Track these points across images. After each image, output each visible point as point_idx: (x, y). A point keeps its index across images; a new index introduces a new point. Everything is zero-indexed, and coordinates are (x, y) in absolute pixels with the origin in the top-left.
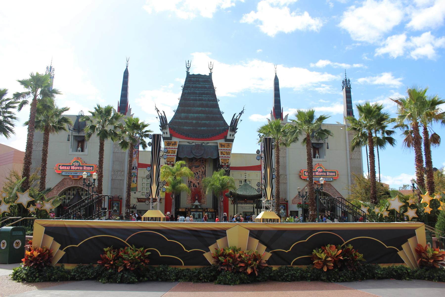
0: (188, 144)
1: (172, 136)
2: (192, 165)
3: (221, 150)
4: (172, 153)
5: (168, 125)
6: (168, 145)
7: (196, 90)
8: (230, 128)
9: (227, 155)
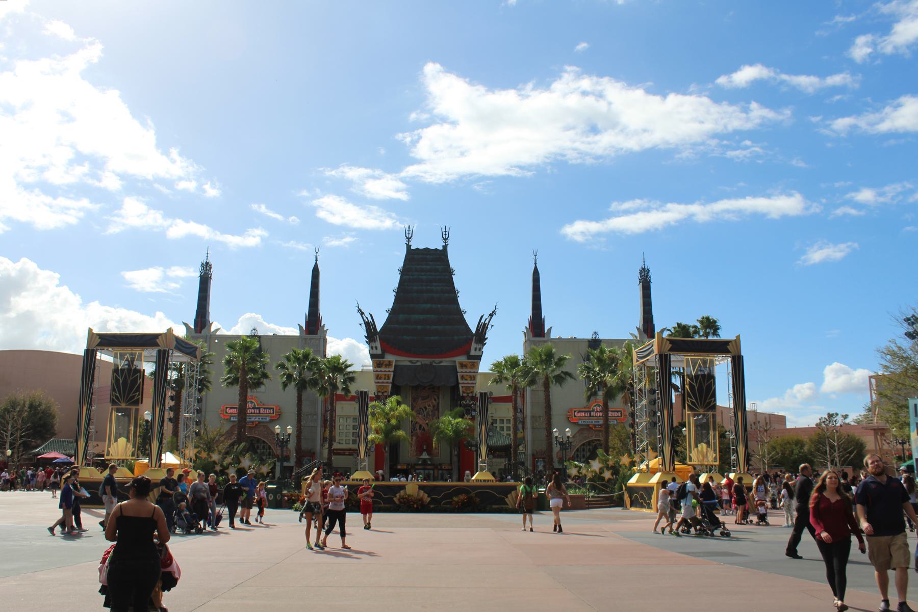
0: (409, 364)
1: (384, 351)
3: (462, 372)
4: (385, 379)
5: (378, 336)
6: (379, 367)
7: (422, 276)
8: (474, 337)
9: (471, 380)
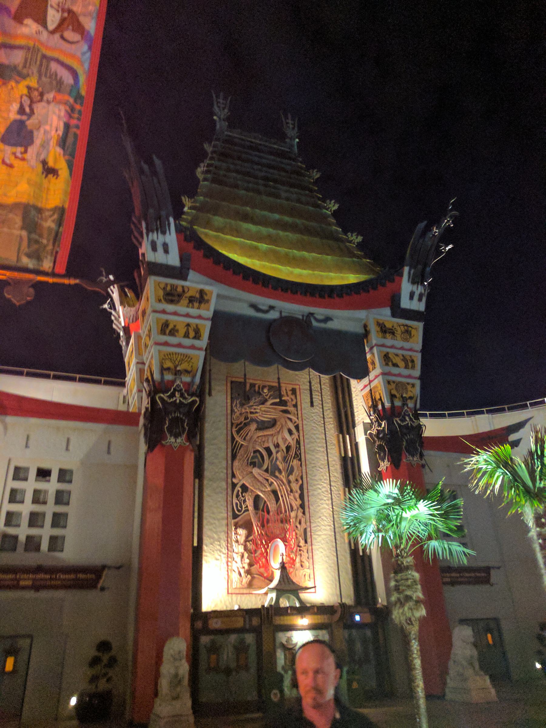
0: (252, 313)
2: (246, 418)
4: (186, 335)
6: (172, 302)
9: (406, 367)
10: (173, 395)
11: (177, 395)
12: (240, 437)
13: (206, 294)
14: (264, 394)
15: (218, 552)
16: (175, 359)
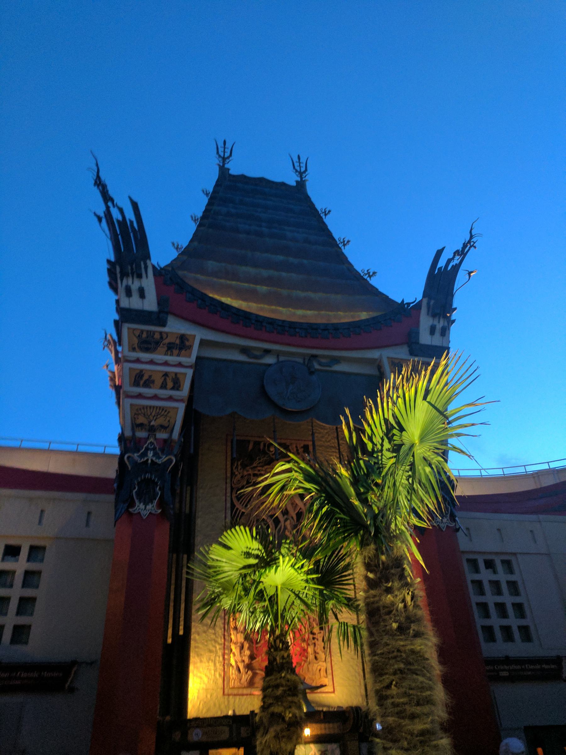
4: (164, 386)
6: (147, 350)
10: (145, 454)
11: (150, 454)
12: (241, 503)
13: (188, 340)
14: (271, 453)
15: (213, 642)
16: (149, 414)
